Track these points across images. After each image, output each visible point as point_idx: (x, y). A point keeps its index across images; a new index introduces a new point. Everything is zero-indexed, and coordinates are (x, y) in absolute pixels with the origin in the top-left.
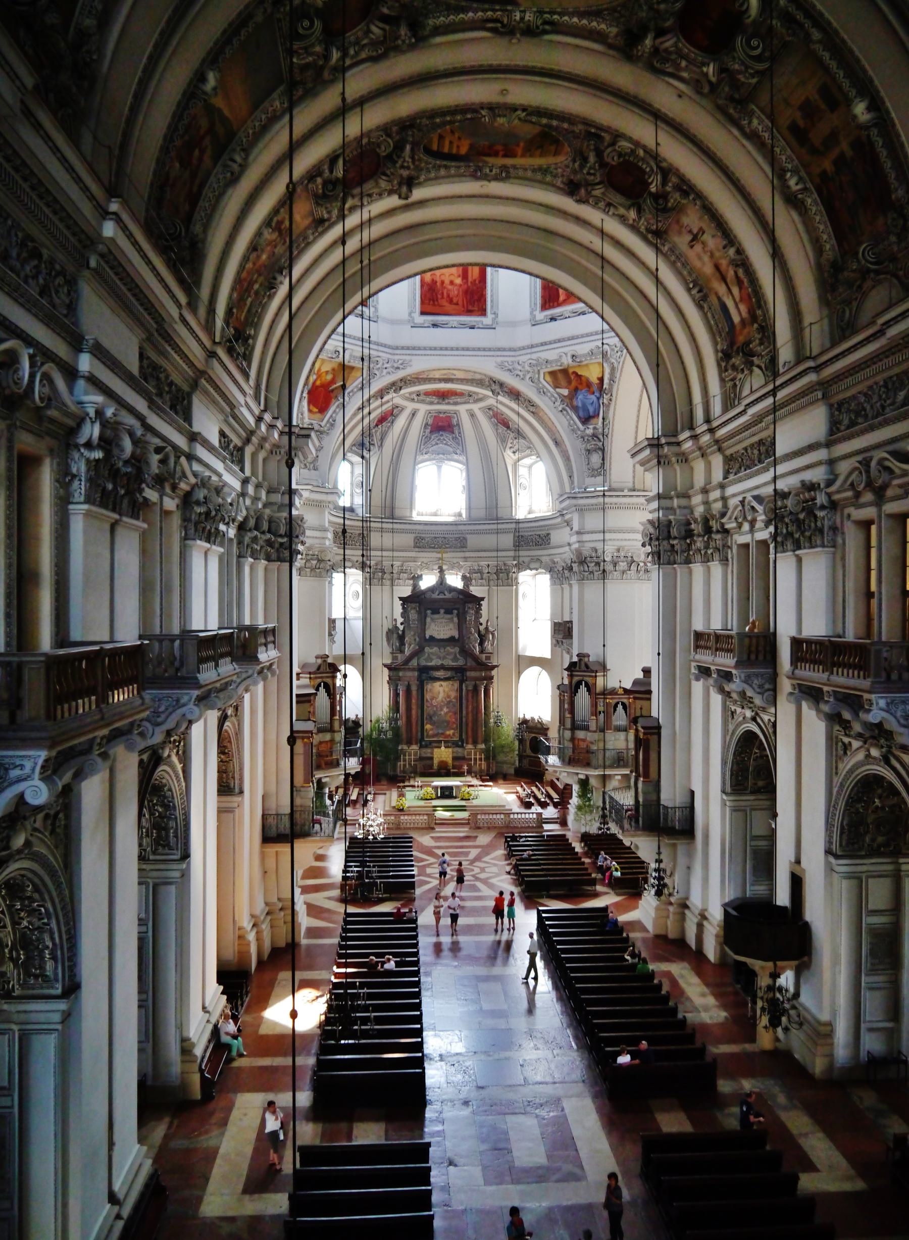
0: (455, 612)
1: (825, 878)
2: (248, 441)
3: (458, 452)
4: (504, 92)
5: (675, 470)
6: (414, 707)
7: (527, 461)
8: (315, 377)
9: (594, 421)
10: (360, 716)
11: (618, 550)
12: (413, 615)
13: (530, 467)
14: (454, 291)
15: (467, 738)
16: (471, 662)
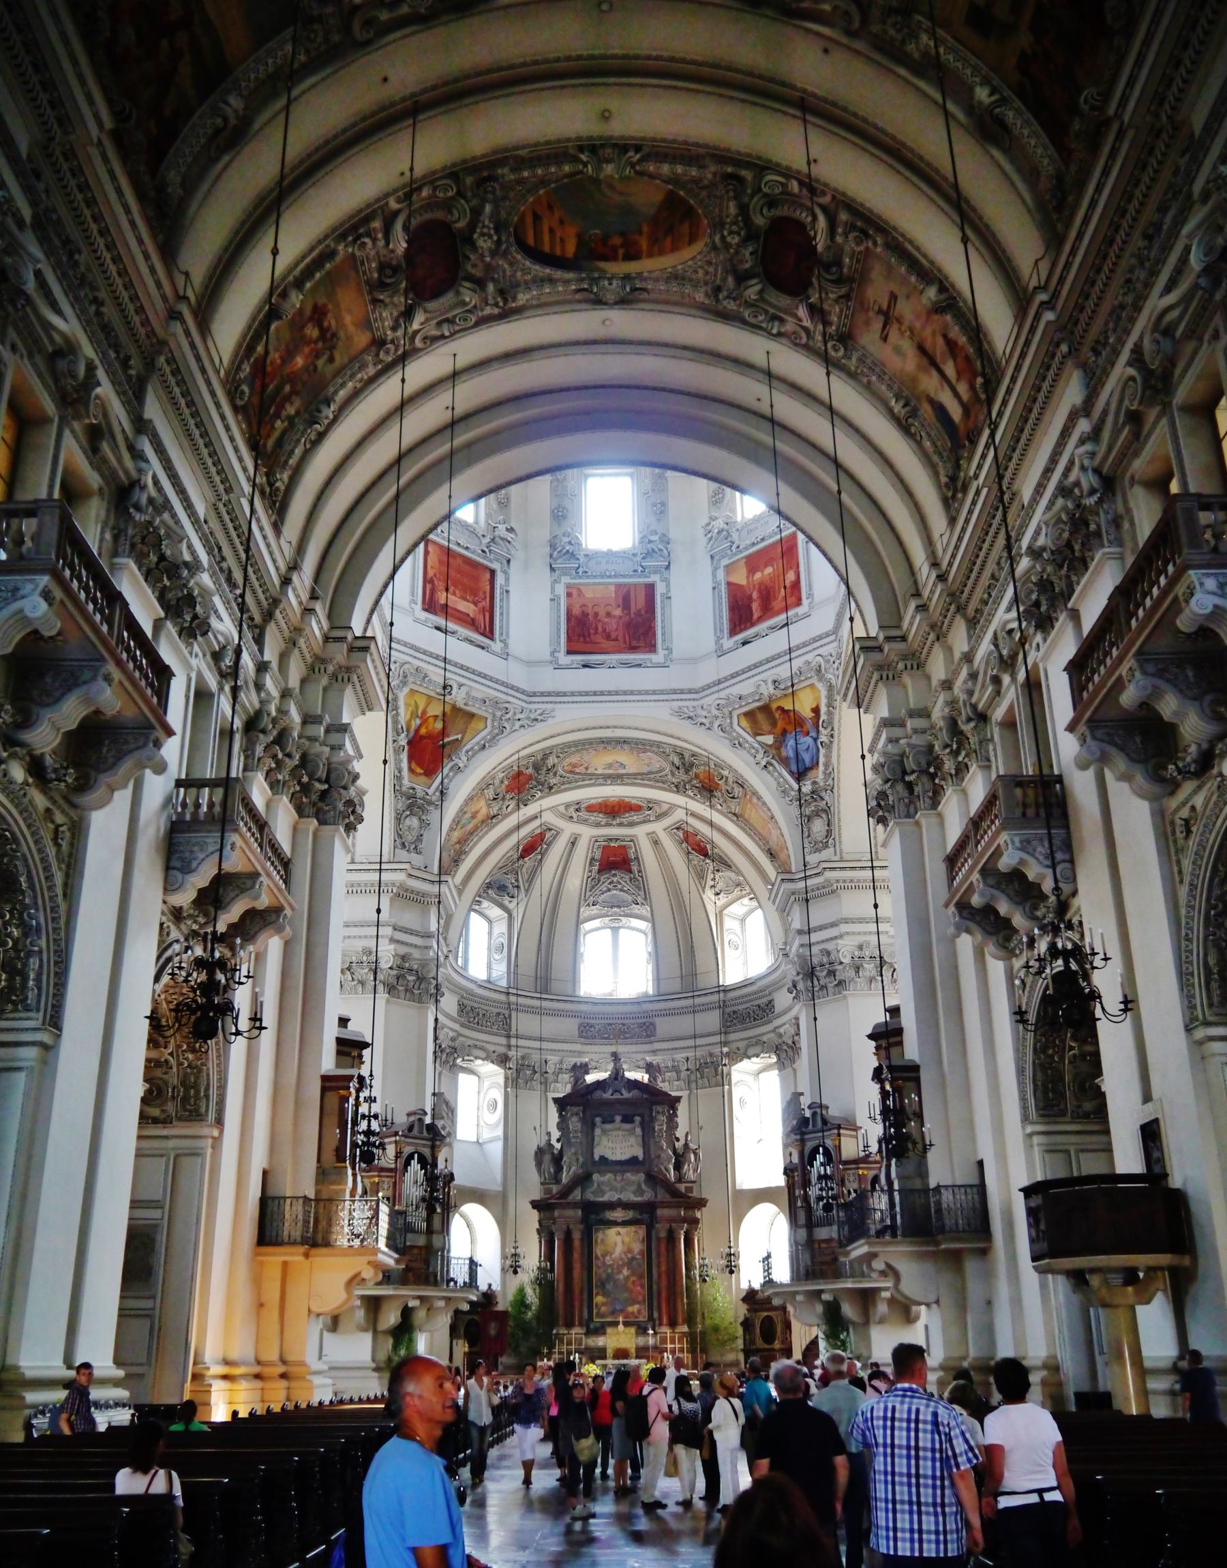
0: (638, 1119)
1: (1193, 1075)
2: (269, 616)
3: (640, 900)
4: (605, 116)
5: (905, 687)
6: (577, 1267)
7: (738, 909)
8: (418, 722)
9: (812, 774)
10: (496, 1287)
11: (860, 947)
12: (575, 1124)
13: (743, 921)
14: (612, 625)
15: (660, 1319)
16: (662, 1195)
